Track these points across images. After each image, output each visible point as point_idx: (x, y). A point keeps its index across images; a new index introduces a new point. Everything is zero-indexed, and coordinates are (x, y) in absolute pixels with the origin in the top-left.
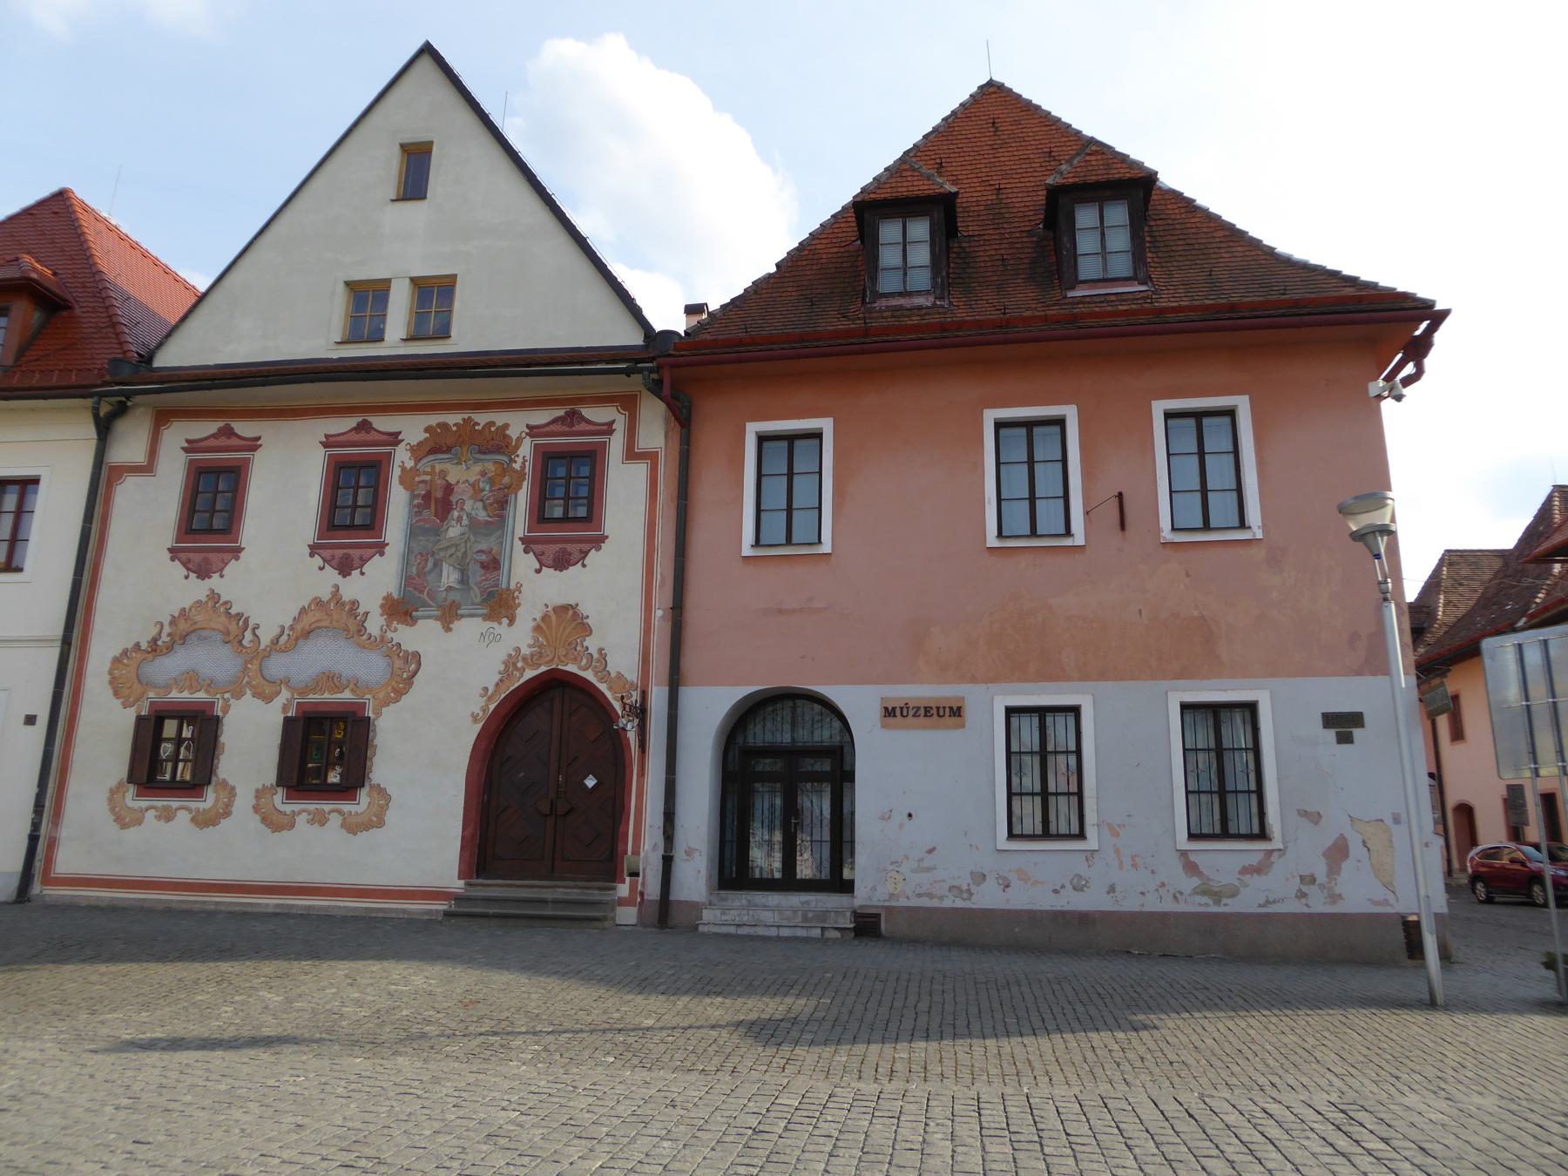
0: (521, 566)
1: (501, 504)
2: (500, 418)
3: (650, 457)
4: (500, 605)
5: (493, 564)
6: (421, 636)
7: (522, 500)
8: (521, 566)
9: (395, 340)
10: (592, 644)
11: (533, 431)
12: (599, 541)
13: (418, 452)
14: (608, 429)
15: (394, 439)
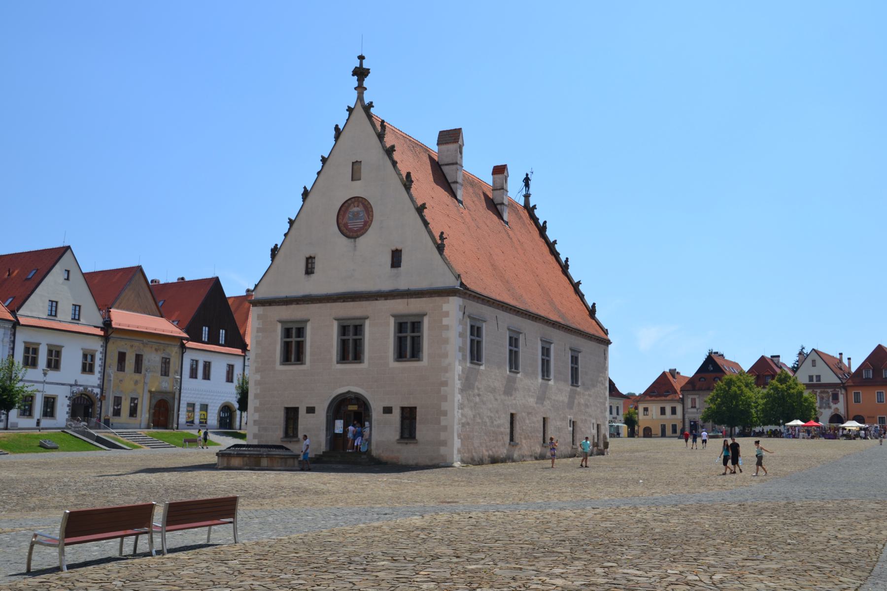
0: (831, 404)
1: (829, 398)
2: (827, 390)
3: (843, 394)
4: (830, 407)
5: (829, 404)
6: (822, 410)
7: (831, 398)
8: (831, 404)
9: (815, 382)
10: (839, 411)
11: (831, 391)
12: (839, 402)
13: (820, 393)
14: (838, 391)
15: (817, 392)
